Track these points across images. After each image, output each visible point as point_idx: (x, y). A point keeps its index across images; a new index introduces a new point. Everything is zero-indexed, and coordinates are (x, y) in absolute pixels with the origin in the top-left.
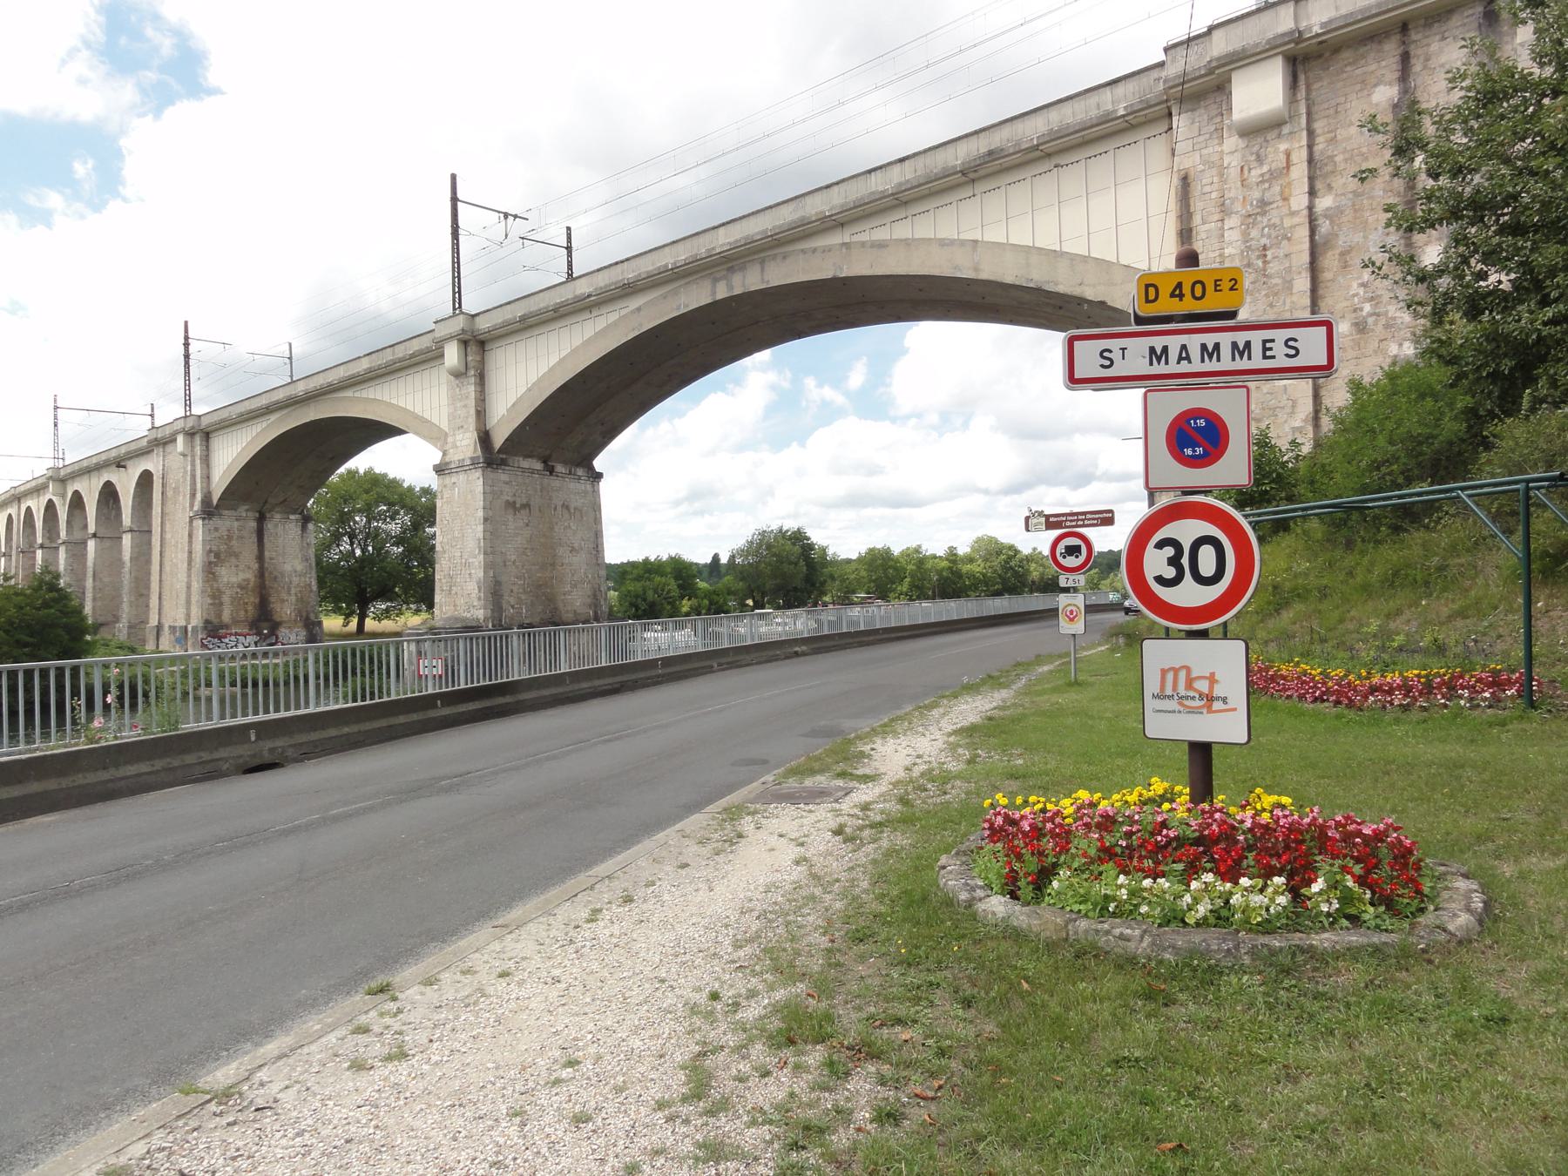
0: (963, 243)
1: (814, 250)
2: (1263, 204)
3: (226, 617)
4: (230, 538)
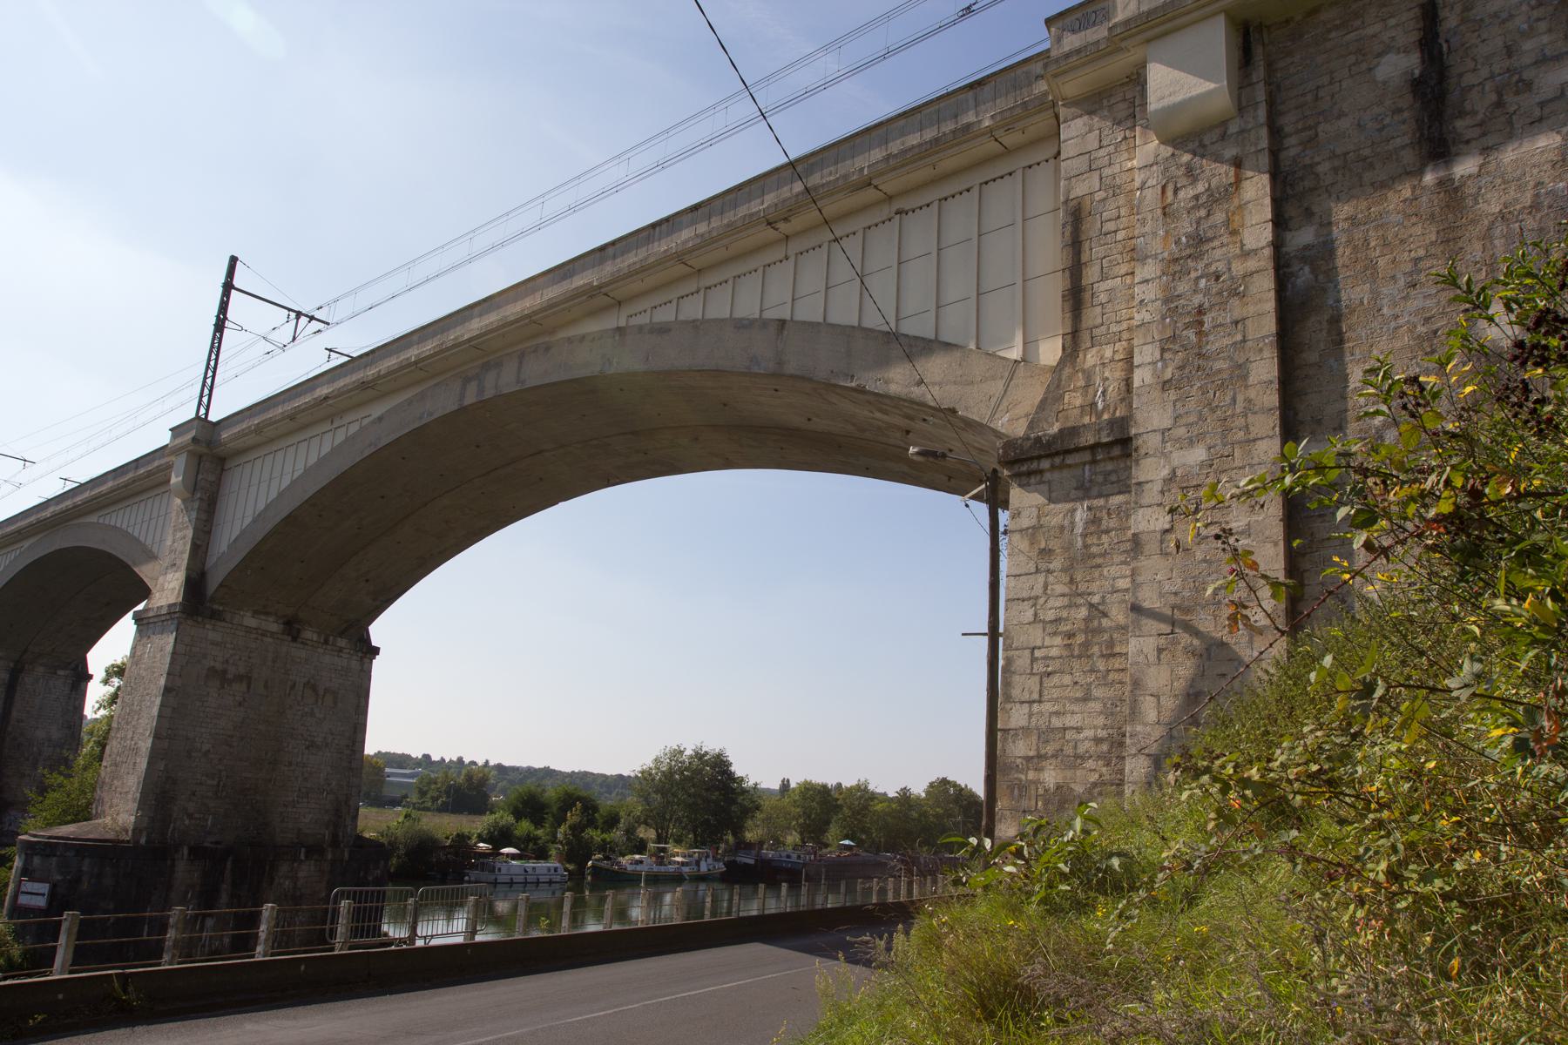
0: (764, 324)
1: (583, 338)
2: (1199, 241)
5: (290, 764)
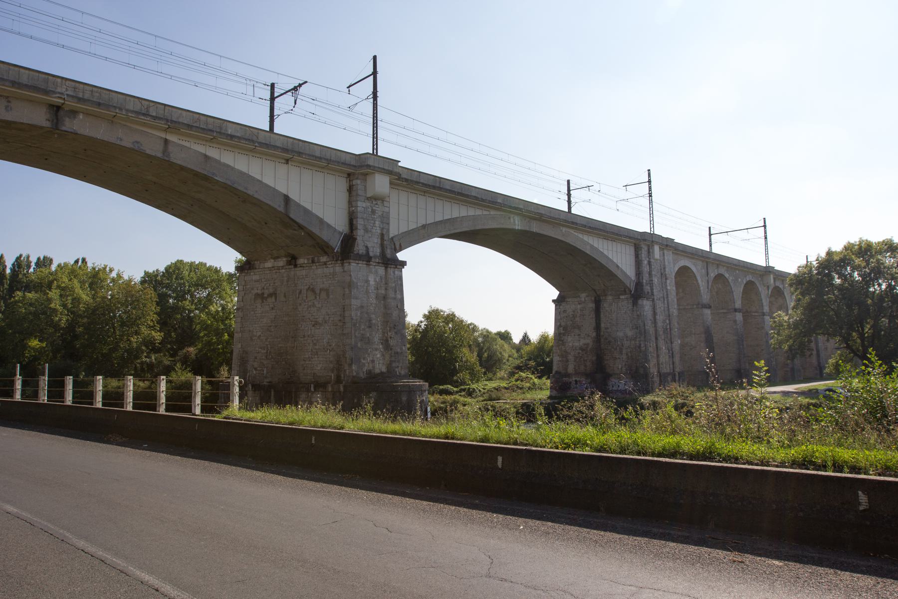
3: (571, 369)
4: (574, 316)
5: (304, 336)
